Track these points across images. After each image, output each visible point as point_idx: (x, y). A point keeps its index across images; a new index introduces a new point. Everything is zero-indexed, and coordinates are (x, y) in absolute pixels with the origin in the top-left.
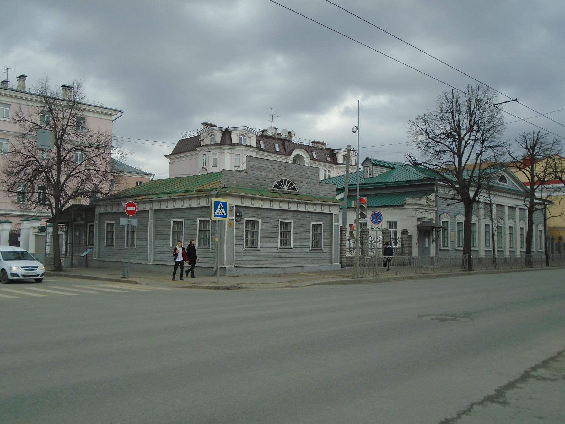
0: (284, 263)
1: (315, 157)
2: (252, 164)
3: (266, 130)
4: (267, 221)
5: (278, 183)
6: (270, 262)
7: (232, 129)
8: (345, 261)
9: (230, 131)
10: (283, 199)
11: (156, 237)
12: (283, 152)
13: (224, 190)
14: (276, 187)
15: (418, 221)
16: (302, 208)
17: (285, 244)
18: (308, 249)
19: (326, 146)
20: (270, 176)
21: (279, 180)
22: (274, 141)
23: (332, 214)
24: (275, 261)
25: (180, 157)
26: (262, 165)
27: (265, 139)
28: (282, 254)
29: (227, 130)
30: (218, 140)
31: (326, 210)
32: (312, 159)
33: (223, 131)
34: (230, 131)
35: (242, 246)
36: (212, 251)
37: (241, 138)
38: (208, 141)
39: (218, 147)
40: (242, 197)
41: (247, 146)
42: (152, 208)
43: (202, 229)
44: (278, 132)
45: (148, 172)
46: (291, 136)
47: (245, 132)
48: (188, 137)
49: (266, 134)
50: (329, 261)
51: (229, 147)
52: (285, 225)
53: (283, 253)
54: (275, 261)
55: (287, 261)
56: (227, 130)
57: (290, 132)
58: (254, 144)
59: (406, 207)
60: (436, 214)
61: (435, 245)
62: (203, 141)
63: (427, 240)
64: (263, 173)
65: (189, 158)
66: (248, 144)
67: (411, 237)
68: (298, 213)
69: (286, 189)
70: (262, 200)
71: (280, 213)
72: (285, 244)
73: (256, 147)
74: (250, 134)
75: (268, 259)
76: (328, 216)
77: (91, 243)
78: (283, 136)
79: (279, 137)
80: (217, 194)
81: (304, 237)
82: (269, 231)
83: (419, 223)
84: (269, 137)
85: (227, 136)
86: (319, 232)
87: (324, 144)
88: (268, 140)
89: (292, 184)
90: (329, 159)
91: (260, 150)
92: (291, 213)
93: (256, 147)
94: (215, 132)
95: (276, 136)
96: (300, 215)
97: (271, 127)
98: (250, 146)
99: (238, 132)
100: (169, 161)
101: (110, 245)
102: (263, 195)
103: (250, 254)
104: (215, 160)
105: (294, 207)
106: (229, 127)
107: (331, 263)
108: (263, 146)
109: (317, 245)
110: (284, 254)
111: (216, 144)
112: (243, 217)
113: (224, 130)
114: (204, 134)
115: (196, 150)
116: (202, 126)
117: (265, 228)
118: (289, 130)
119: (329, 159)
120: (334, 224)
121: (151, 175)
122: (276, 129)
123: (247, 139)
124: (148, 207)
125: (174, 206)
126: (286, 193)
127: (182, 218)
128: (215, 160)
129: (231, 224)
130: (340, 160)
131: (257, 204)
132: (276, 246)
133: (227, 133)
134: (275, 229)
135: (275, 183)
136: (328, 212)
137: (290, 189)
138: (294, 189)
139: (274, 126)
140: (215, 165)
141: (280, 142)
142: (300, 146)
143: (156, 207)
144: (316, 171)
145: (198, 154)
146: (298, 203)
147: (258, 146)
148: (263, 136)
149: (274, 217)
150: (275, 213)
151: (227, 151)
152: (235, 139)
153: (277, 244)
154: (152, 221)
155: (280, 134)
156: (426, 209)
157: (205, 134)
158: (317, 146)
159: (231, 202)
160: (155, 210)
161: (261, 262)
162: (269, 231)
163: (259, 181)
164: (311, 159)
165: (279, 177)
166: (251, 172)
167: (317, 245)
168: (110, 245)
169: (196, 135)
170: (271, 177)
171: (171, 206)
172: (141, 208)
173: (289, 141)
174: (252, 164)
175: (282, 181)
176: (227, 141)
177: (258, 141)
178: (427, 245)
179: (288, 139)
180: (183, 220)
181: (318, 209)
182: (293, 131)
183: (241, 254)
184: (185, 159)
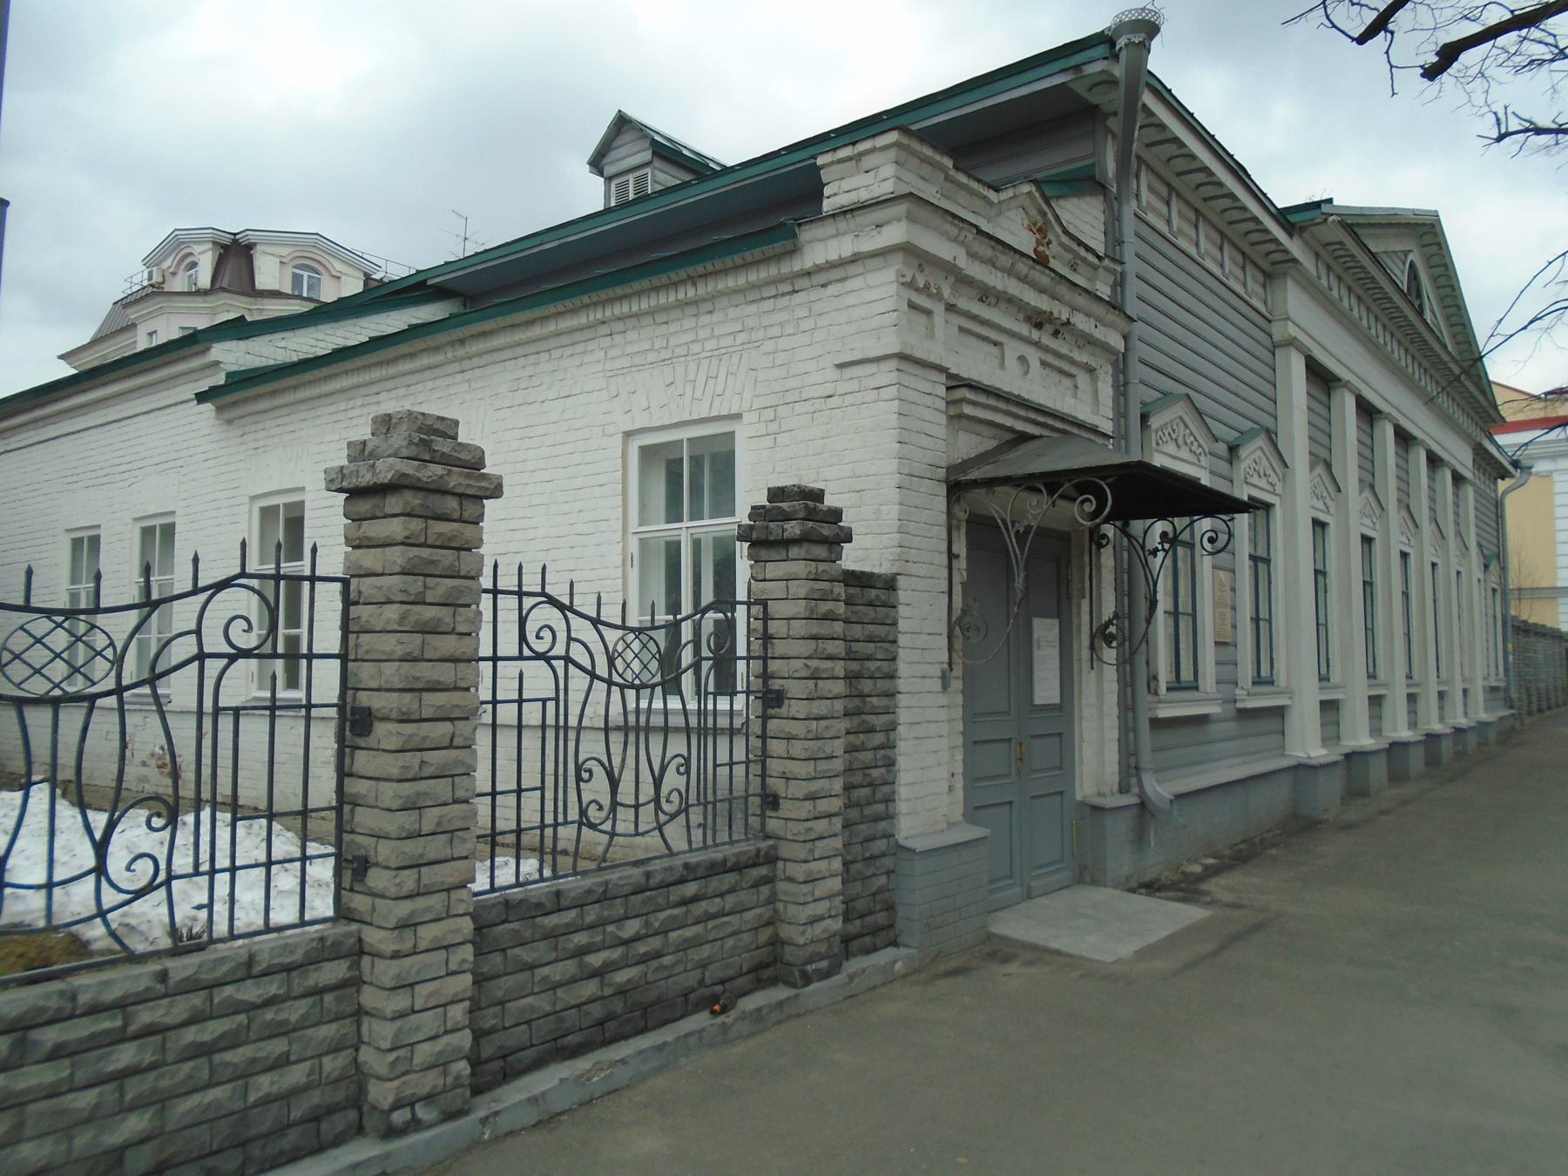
7: (252, 237)
9: (250, 247)
15: (956, 419)
29: (235, 241)
33: (224, 247)
34: (250, 247)
37: (297, 280)
38: (179, 284)
56: (235, 241)
59: (822, 246)
60: (1121, 390)
61: (1111, 674)
63: (1046, 631)
67: (872, 593)
74: (339, 266)
83: (969, 445)
99: (285, 251)
111: (200, 293)
113: (227, 240)
133: (236, 253)
156: (1038, 320)
157: (168, 262)
178: (1046, 690)
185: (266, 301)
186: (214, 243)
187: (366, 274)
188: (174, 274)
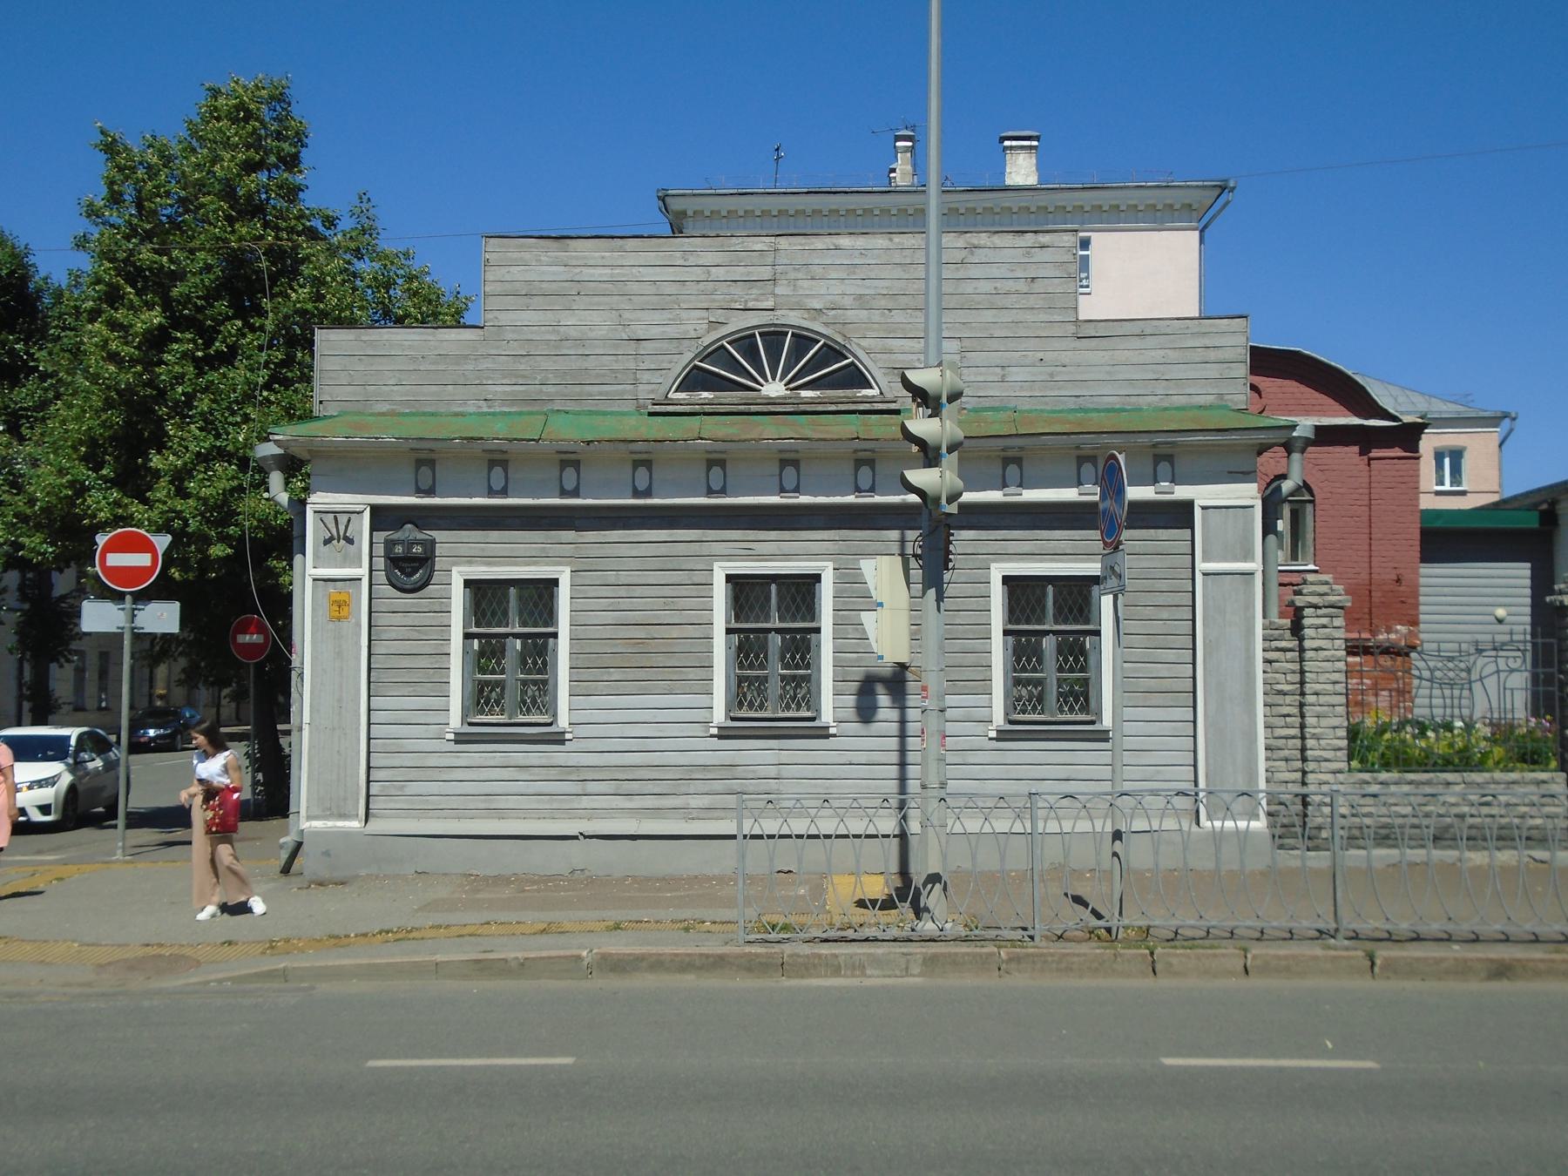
2: (516, 273)
6: (650, 802)
14: (695, 379)
18: (979, 728)
20: (648, 324)
24: (695, 802)
26: (588, 273)
28: (739, 758)
53: (757, 754)
54: (695, 802)
64: (595, 318)
69: (774, 389)
82: (640, 632)
110: (770, 757)
112: (439, 563)
120: (1201, 566)
126: (772, 410)
129: (340, 605)
138: (855, 378)
153: (701, 700)
161: (586, 802)
162: (640, 632)
163: (562, 364)
165: (714, 325)
166: (505, 319)
170: (655, 332)
174: (516, 273)
175: (746, 343)
183: (433, 761)
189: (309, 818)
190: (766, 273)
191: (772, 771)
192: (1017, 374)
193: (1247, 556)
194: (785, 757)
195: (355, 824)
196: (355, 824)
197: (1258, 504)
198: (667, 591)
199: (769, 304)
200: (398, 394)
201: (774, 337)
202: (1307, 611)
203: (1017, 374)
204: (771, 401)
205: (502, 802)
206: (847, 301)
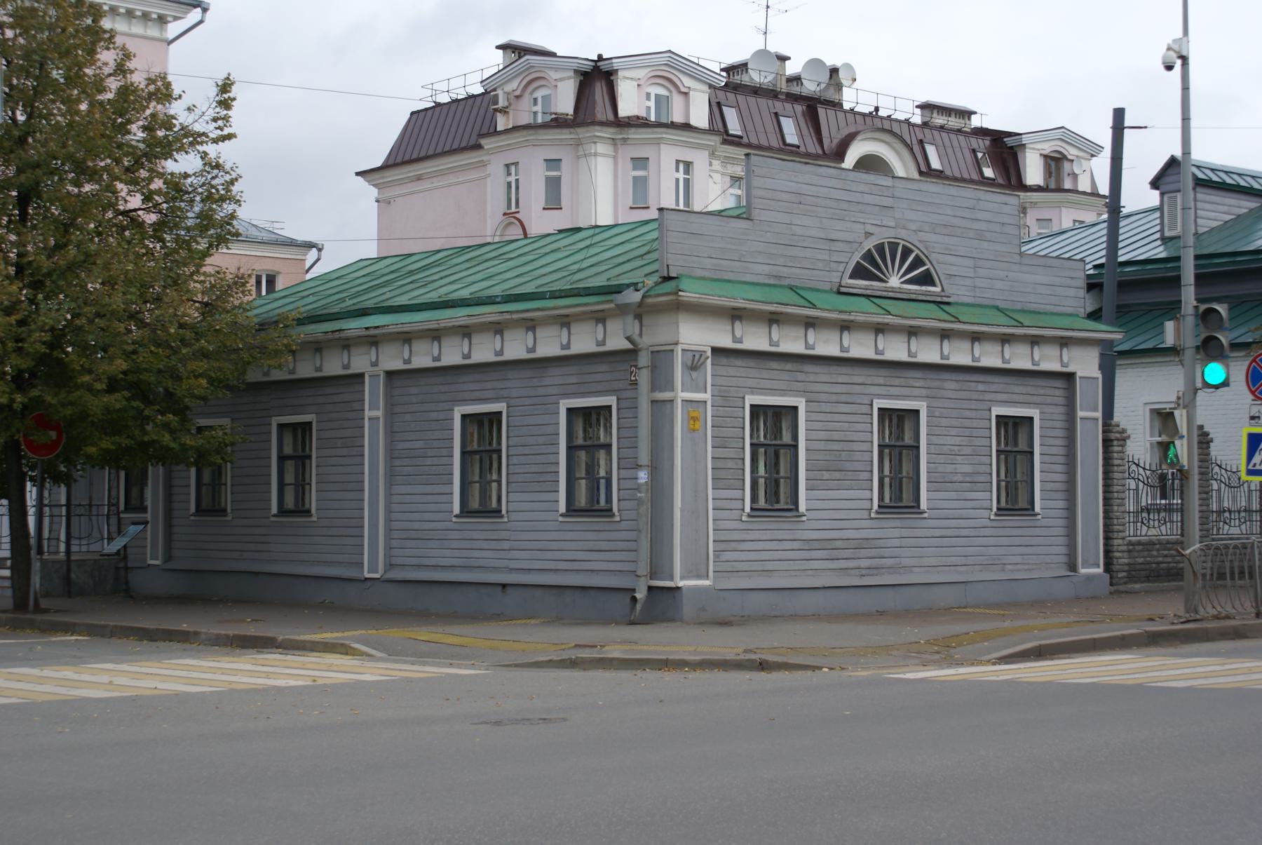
0: (891, 569)
1: (936, 164)
3: (743, 67)
4: (828, 408)
5: (868, 256)
7: (616, 64)
8: (1122, 559)
10: (888, 319)
11: (391, 475)
12: (813, 147)
13: (670, 286)
14: (859, 272)
16: (960, 355)
17: (900, 497)
18: (985, 513)
19: (976, 122)
21: (869, 244)
22: (778, 106)
23: (1070, 377)
25: (419, 178)
27: (741, 98)
30: (565, 103)
31: (1049, 360)
32: (927, 172)
35: (738, 505)
36: (624, 525)
39: (565, 134)
40: (736, 315)
41: (673, 126)
42: (375, 364)
43: (580, 441)
44: (792, 68)
45: (301, 237)
46: (839, 87)
47: (670, 70)
48: (444, 99)
49: (745, 79)
50: (1063, 559)
51: (607, 133)
52: (898, 422)
53: (893, 529)
55: (906, 562)
57: (834, 71)
58: (700, 116)
62: (504, 111)
65: (452, 179)
66: (678, 118)
68: (945, 376)
69: (894, 281)
70: (810, 323)
71: (878, 376)
72: (900, 497)
73: (711, 131)
74: (688, 82)
75: (835, 553)
76: (1059, 383)
77: (135, 502)
78: (810, 87)
79: (795, 89)
80: (640, 304)
81: (967, 469)
84: (756, 91)
85: (599, 89)
86: (1022, 446)
87: (967, 114)
88: (752, 100)
89: (918, 262)
90: (988, 172)
91: (725, 142)
92: (918, 374)
93: (711, 131)
94: (554, 75)
95: (783, 86)
96: (950, 383)
97: (762, 54)
98: (687, 127)
99: (641, 73)
100: (373, 192)
101: (210, 508)
102: (814, 306)
103: (768, 535)
104: (553, 186)
105: (929, 352)
106: (600, 57)
107: (1073, 567)
108: (734, 127)
109: (1015, 501)
111: (559, 122)
113: (588, 67)
114: (509, 88)
115: (479, 147)
116: (498, 58)
117: (822, 435)
118: (830, 62)
119: (988, 172)
120: (1080, 414)
121: (309, 245)
122: (783, 59)
123: (677, 101)
124: (360, 362)
125: (437, 359)
127: (497, 399)
128: (553, 186)
129: (694, 419)
130: (1033, 173)
131: (792, 342)
132: (866, 504)
133: (597, 77)
134: (862, 436)
135: (857, 257)
136: (1055, 366)
137: (910, 282)
139: (772, 48)
140: (553, 202)
141: (799, 108)
142: (875, 123)
143: (392, 359)
144: (1007, 209)
145: (483, 165)
146: (945, 335)
147: (718, 128)
148: (734, 84)
149: (857, 389)
150: (859, 375)
151: (601, 148)
152: (630, 101)
153: (867, 494)
154: (379, 413)
155: (796, 79)
157: (514, 85)
158: (939, 120)
159: (696, 335)
160: (389, 374)
162: (836, 446)
164: (921, 173)
165: (868, 235)
167: (1015, 501)
168: (210, 508)
169: (478, 90)
171: (484, 351)
172: (333, 365)
173: (837, 105)
175: (880, 248)
176: (601, 110)
177: (716, 108)
179: (831, 95)
180: (500, 406)
181: (1020, 358)
182: (848, 66)
183: (737, 536)
184: (436, 182)
185: (633, 130)
186: (575, 71)
187: (711, 86)
188: (518, 97)
189: (682, 578)
190: (887, 202)
191: (897, 542)
192: (999, 285)
193: (1096, 410)
194: (905, 532)
195: (707, 583)
196: (707, 583)
197: (1100, 376)
198: (850, 418)
199: (893, 224)
200: (708, 263)
201: (893, 246)
202: (1115, 443)
203: (999, 285)
204: (893, 290)
205: (770, 566)
206: (927, 228)
